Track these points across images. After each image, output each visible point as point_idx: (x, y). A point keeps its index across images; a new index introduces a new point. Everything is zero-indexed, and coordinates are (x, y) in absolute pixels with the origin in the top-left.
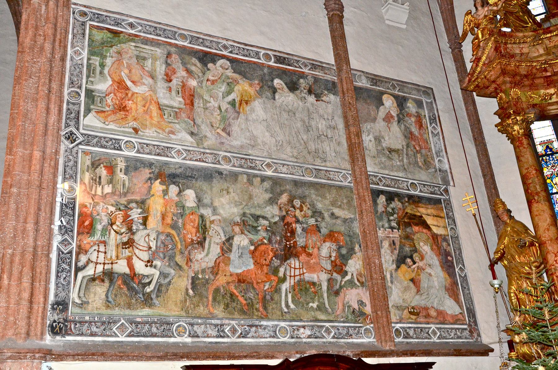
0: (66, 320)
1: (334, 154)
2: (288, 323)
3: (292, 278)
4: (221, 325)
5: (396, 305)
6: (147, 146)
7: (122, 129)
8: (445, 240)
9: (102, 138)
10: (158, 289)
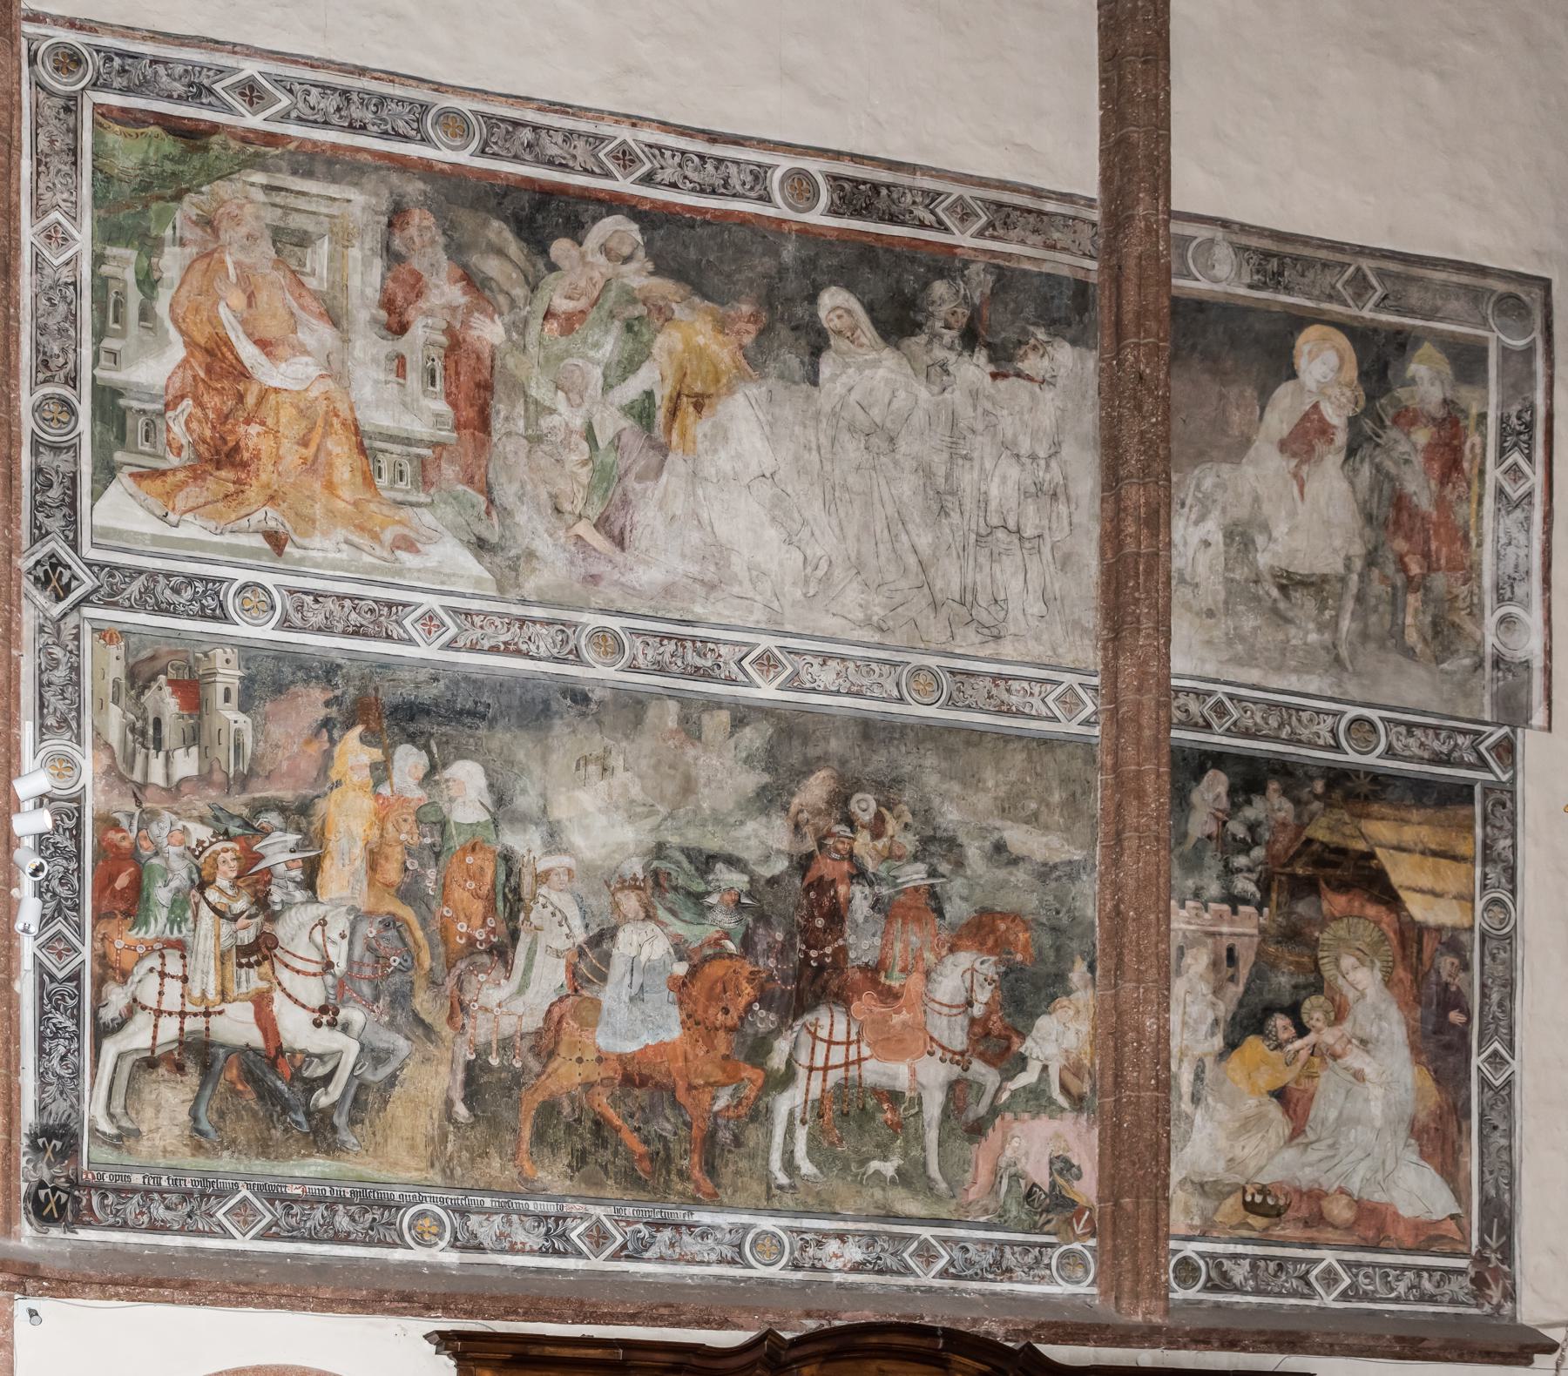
0: (74, 1183)
1: (1037, 608)
3: (817, 1077)
4: (557, 1219)
5: (1196, 1179)
6: (316, 601)
7: (228, 539)
9: (161, 578)
10: (355, 1099)
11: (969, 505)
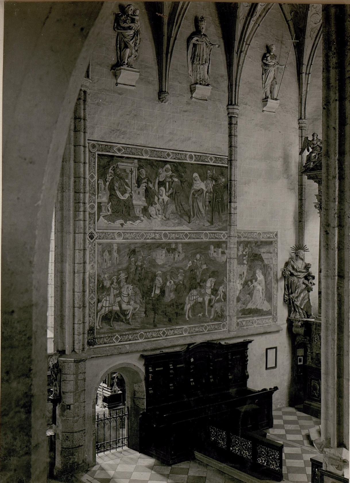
0: (94, 338)
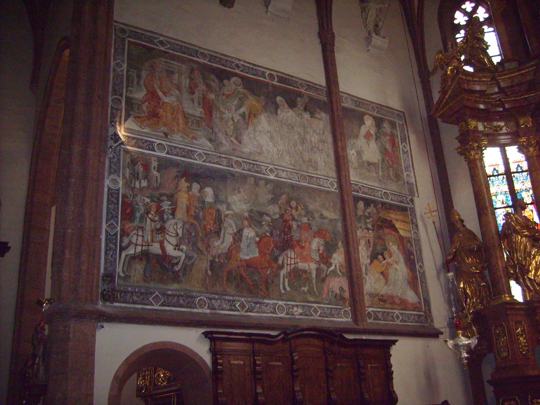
0: (114, 290)
1: (323, 164)
2: (284, 302)
3: (289, 266)
6: (175, 149)
7: (155, 133)
8: (409, 241)
10: (184, 269)
11: (308, 141)
